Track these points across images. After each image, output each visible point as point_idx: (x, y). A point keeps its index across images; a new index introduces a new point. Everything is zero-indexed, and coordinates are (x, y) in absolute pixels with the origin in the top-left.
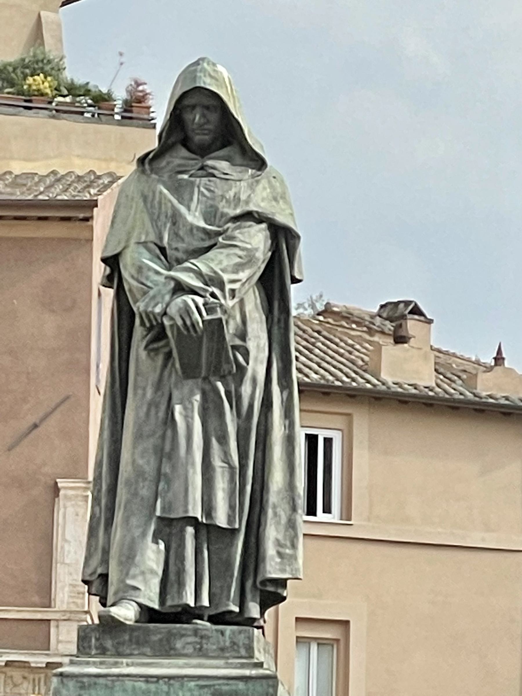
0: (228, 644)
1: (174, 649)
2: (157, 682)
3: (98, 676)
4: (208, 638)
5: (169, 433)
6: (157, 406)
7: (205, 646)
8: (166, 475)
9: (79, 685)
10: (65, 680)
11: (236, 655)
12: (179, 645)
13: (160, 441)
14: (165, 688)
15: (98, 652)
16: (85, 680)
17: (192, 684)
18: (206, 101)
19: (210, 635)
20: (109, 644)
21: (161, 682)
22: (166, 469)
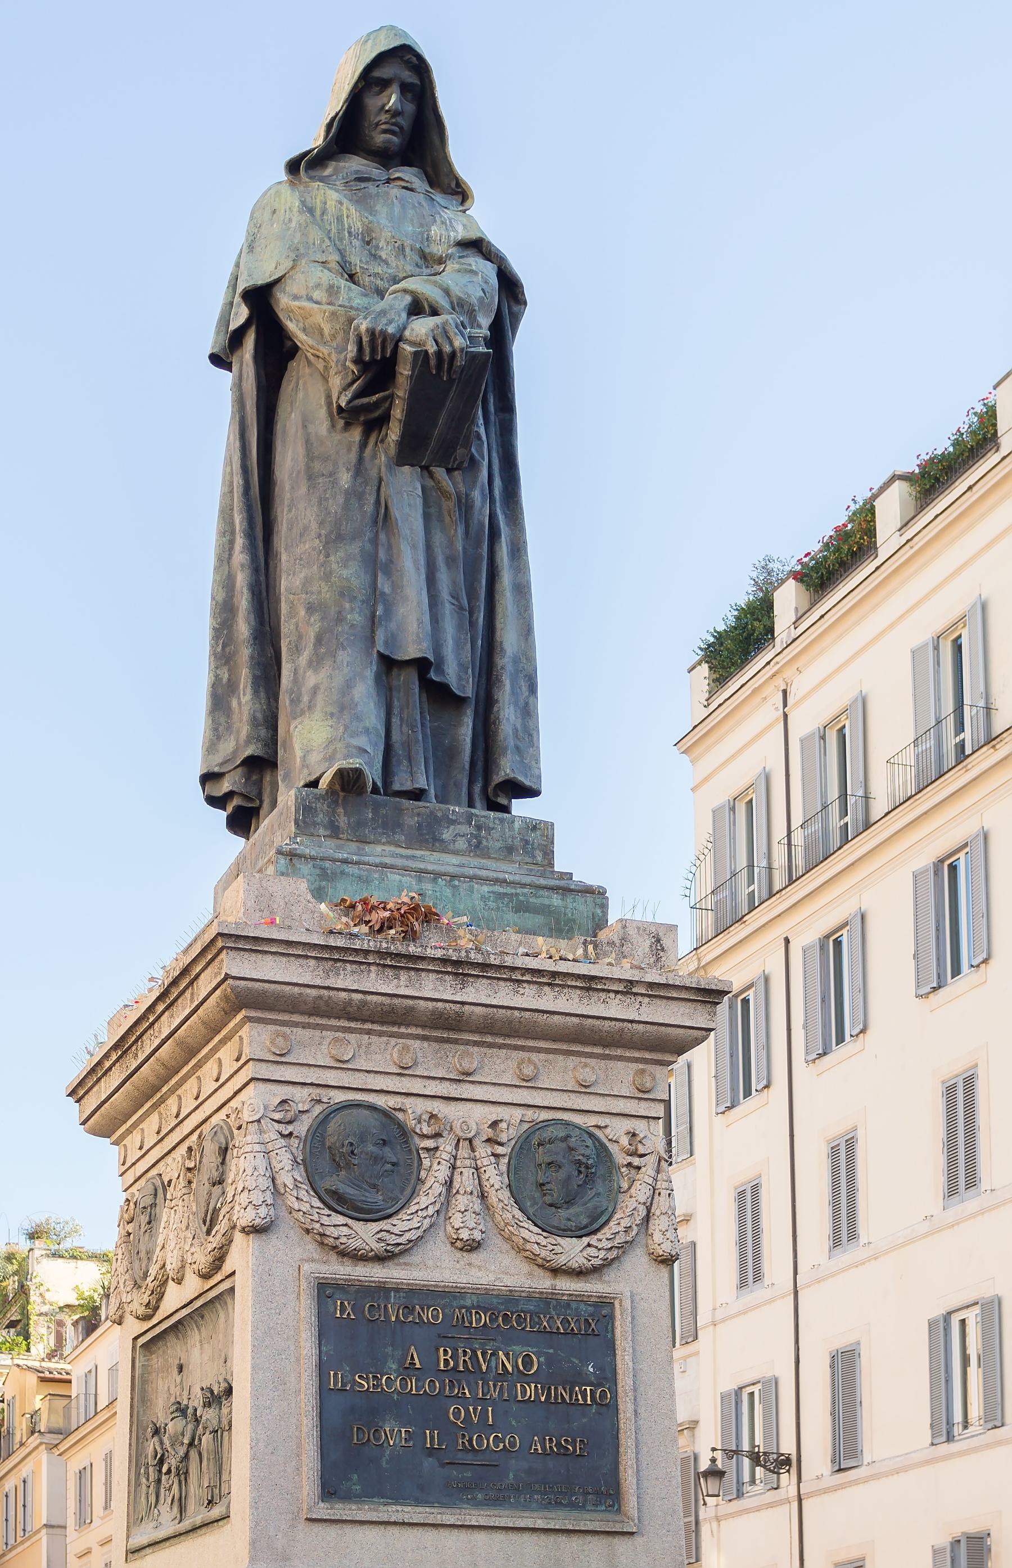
0: (517, 842)
2: (435, 880)
3: (345, 861)
4: (489, 829)
5: (382, 537)
6: (361, 497)
7: (484, 842)
8: (383, 594)
9: (318, 871)
10: (295, 860)
11: (529, 860)
12: (447, 835)
13: (368, 546)
14: (448, 892)
15: (328, 833)
16: (327, 864)
17: (485, 889)
19: (491, 825)
20: (343, 821)
22: (384, 585)
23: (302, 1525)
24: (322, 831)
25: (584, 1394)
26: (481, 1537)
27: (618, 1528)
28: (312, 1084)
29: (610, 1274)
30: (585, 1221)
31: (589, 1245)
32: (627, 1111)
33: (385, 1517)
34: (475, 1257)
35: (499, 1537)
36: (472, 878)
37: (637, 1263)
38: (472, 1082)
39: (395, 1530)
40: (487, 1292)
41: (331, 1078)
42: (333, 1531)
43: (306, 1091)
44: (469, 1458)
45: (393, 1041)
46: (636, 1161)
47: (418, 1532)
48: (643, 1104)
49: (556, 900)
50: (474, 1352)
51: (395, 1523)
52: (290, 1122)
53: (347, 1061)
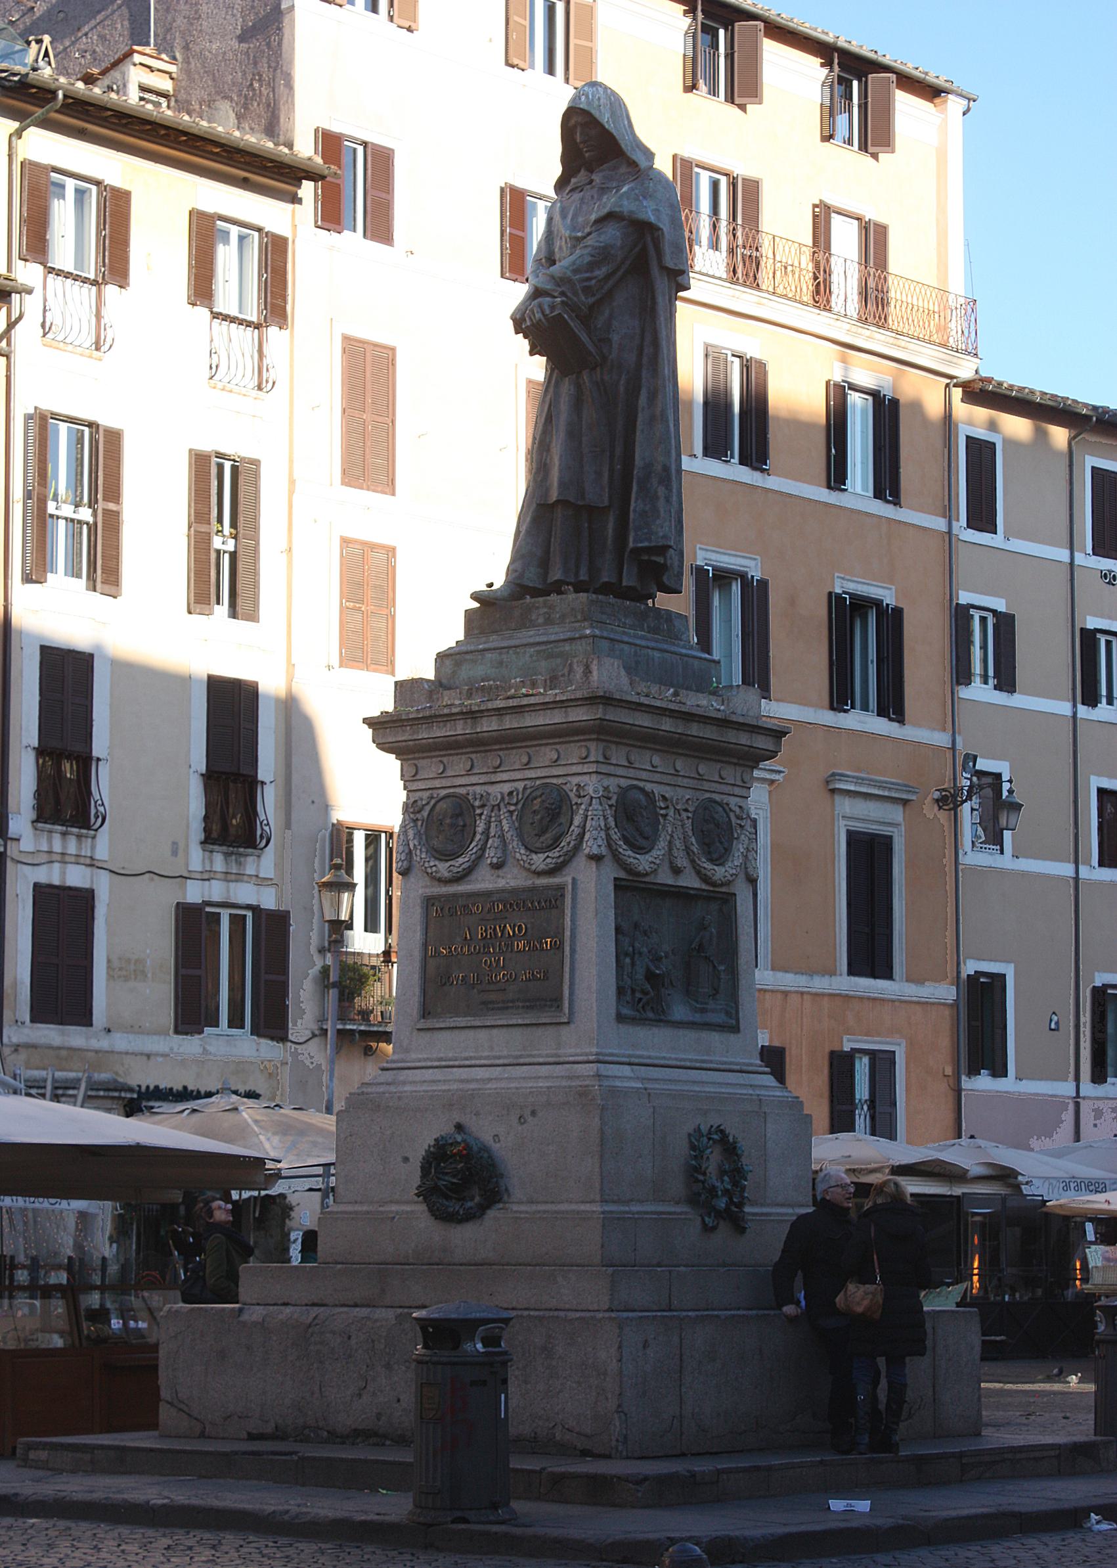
1: (531, 621)
3: (467, 653)
18: (580, 119)
21: (511, 652)
23: (415, 1032)
24: (476, 632)
25: (546, 942)
26: (495, 1031)
27: (558, 1021)
28: (429, 789)
29: (566, 870)
30: (551, 842)
31: (548, 857)
32: (577, 771)
33: (448, 1025)
34: (500, 872)
35: (504, 1030)
36: (526, 645)
37: (580, 862)
38: (502, 771)
39: (457, 1032)
40: (502, 891)
41: (437, 783)
42: (428, 1035)
43: (428, 793)
44: (492, 987)
45: (463, 757)
46: (579, 801)
47: (467, 1031)
48: (586, 766)
49: (567, 647)
50: (495, 928)
51: (456, 1028)
52: (419, 812)
53: (442, 773)
